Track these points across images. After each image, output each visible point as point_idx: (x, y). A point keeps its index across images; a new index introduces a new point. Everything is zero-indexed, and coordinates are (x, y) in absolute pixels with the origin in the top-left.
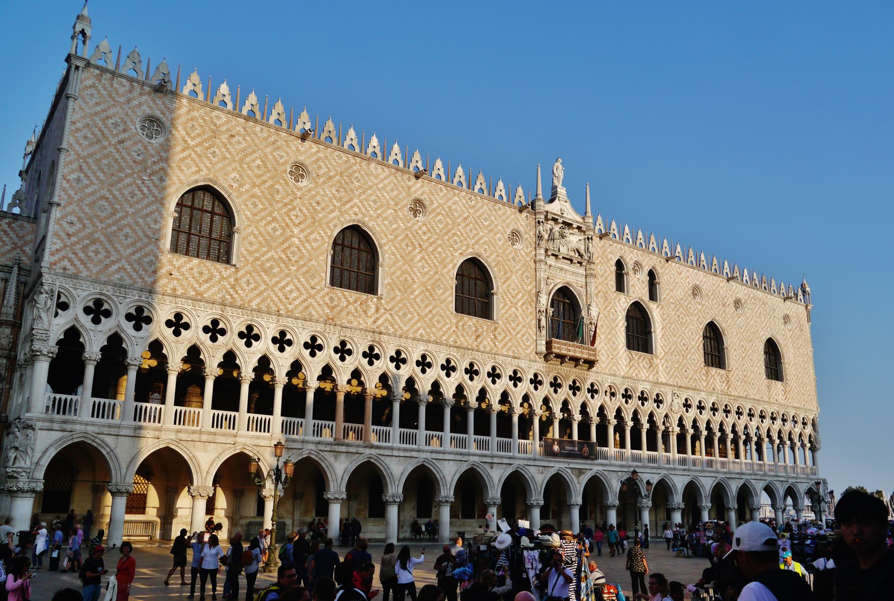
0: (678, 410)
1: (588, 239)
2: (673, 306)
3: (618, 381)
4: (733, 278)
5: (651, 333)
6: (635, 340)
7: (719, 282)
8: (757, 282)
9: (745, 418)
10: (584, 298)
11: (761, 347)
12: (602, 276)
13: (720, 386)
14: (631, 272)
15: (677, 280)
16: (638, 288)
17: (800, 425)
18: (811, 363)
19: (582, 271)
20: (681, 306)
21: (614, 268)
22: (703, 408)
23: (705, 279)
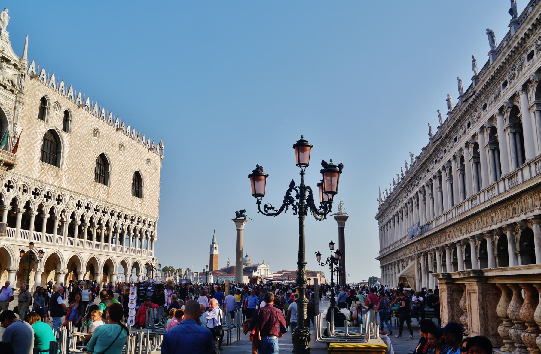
0: (72, 208)
1: (22, 75)
2: (78, 138)
3: (30, 182)
4: (120, 129)
5: (60, 153)
6: (48, 155)
7: (113, 130)
9: (115, 218)
10: (12, 117)
11: (131, 176)
12: (29, 105)
13: (102, 196)
14: (52, 108)
15: (84, 122)
16: (55, 120)
17: (147, 226)
19: (13, 97)
20: (84, 139)
21: (39, 102)
22: (89, 208)
23: (103, 126)
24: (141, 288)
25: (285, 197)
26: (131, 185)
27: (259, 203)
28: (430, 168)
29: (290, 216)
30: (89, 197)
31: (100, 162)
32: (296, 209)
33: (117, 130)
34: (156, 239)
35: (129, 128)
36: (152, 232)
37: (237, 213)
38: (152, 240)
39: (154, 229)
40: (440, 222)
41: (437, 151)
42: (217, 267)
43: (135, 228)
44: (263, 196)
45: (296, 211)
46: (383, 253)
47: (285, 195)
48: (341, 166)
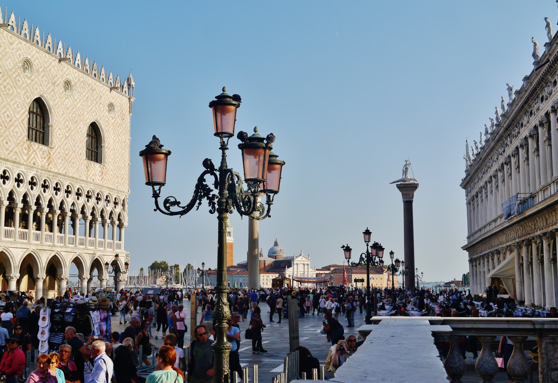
4: (65, 59)
7: (52, 60)
8: (88, 68)
11: (85, 129)
13: (40, 162)
15: (7, 50)
17: (112, 205)
18: (128, 150)
22: (21, 181)
23: (37, 55)
24: (56, 311)
25: (197, 186)
26: (84, 145)
27: (156, 195)
28: (534, 110)
29: (204, 216)
30: (21, 164)
31: (35, 111)
32: (214, 204)
33: (60, 61)
34: (126, 224)
35: (79, 57)
38: (120, 226)
39: (124, 209)
40: (547, 194)
41: (543, 82)
42: (232, 261)
44: (162, 184)
45: (213, 207)
46: (472, 239)
47: (196, 182)
48: (270, 138)
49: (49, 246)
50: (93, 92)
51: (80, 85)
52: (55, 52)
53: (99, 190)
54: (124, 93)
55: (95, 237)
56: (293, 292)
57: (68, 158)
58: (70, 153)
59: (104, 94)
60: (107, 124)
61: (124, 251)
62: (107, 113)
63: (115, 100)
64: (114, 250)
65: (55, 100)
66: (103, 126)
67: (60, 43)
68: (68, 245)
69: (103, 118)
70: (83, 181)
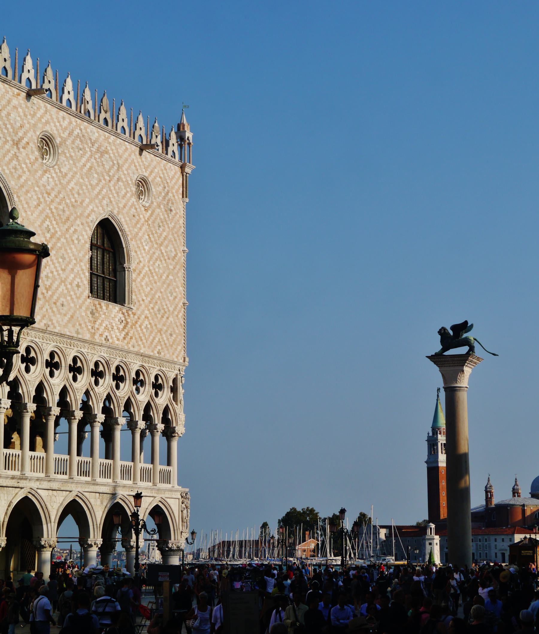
4: (38, 92)
26: (86, 266)
33: (29, 95)
34: (180, 429)
35: (69, 85)
36: (166, 410)
37: (442, 332)
39: (175, 398)
43: (109, 398)
49: (13, 478)
50: (102, 156)
51: (73, 142)
52: (17, 78)
53: (119, 359)
54: (169, 156)
55: (92, 455)
56: (502, 574)
57: (52, 296)
58: (55, 285)
59: (127, 160)
60: (134, 222)
61: (177, 487)
62: (134, 199)
63: (152, 172)
64: (154, 484)
65: (20, 177)
66: (125, 227)
67: (29, 59)
68: (53, 476)
69: (125, 211)
70: (85, 341)
